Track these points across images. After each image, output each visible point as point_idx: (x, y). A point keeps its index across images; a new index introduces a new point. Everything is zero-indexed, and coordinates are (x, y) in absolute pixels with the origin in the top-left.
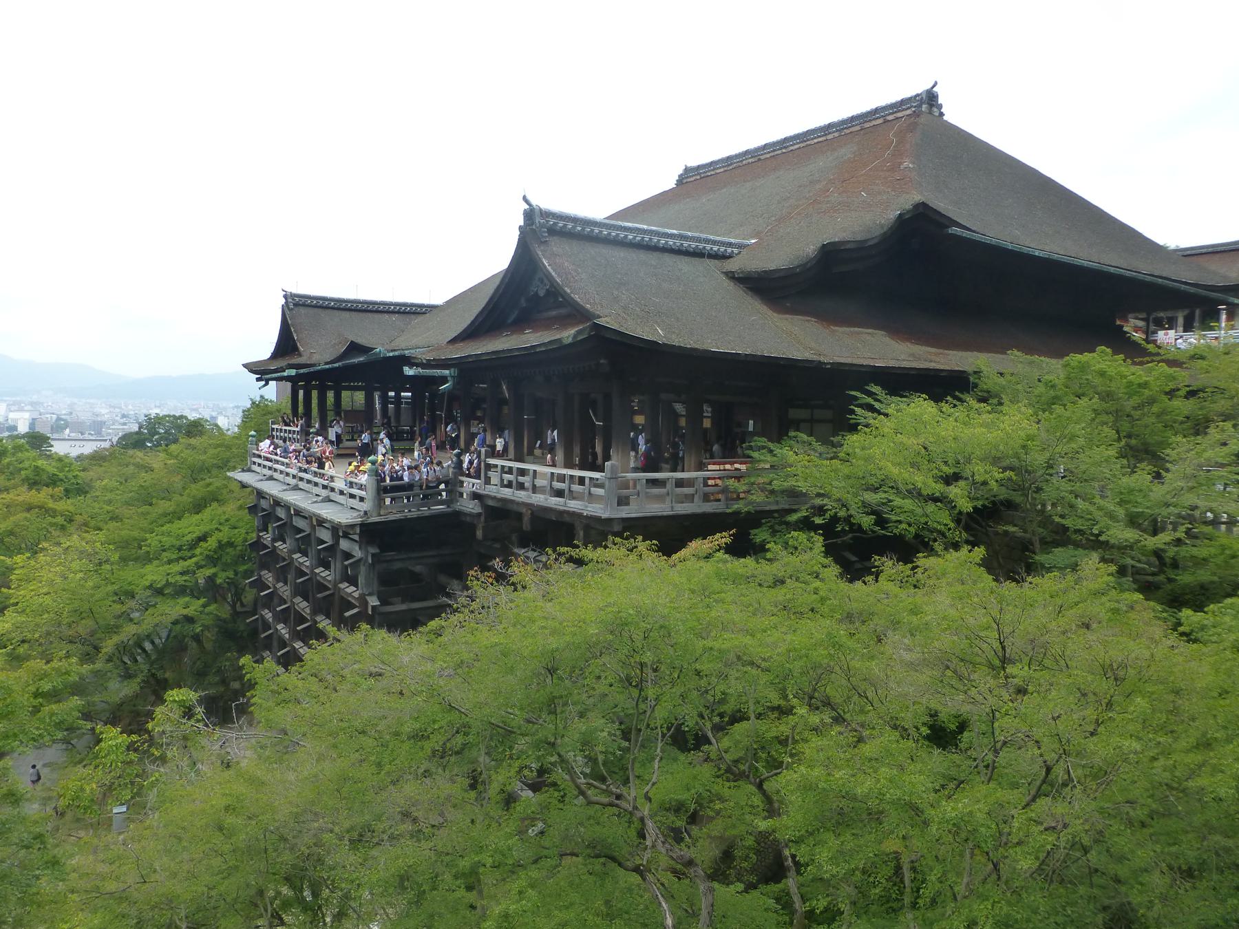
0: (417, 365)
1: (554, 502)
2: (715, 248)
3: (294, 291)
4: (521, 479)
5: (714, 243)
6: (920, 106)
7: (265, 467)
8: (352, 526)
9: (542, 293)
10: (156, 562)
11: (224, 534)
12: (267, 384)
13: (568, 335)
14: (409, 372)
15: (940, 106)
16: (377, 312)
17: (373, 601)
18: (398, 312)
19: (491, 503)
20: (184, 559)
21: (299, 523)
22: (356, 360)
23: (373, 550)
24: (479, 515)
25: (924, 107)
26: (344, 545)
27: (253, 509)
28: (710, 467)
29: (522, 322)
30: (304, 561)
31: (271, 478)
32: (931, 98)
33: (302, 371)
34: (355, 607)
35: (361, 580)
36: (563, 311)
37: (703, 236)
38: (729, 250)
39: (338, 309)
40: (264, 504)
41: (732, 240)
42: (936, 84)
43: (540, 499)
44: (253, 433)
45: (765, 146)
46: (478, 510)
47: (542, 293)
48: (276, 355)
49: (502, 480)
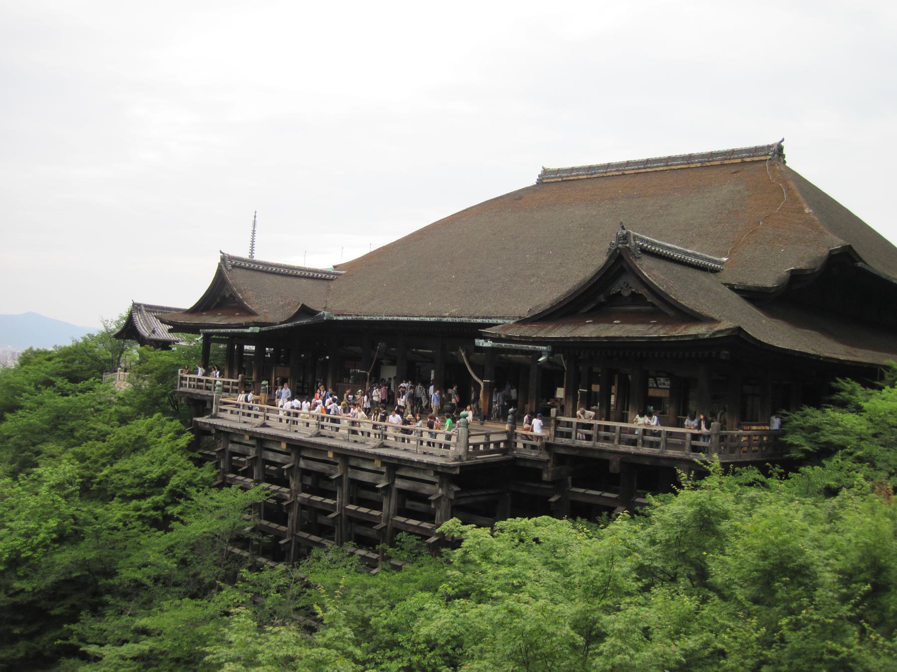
1: (646, 450)
5: (709, 260)
7: (243, 414)
8: (454, 468)
9: (626, 294)
14: (480, 343)
15: (784, 156)
16: (296, 276)
19: (562, 451)
22: (304, 321)
23: (456, 489)
24: (548, 461)
26: (399, 484)
28: (745, 428)
31: (264, 425)
33: (264, 329)
39: (266, 272)
42: (783, 140)
43: (632, 449)
45: (628, 163)
46: (545, 456)
47: (626, 294)
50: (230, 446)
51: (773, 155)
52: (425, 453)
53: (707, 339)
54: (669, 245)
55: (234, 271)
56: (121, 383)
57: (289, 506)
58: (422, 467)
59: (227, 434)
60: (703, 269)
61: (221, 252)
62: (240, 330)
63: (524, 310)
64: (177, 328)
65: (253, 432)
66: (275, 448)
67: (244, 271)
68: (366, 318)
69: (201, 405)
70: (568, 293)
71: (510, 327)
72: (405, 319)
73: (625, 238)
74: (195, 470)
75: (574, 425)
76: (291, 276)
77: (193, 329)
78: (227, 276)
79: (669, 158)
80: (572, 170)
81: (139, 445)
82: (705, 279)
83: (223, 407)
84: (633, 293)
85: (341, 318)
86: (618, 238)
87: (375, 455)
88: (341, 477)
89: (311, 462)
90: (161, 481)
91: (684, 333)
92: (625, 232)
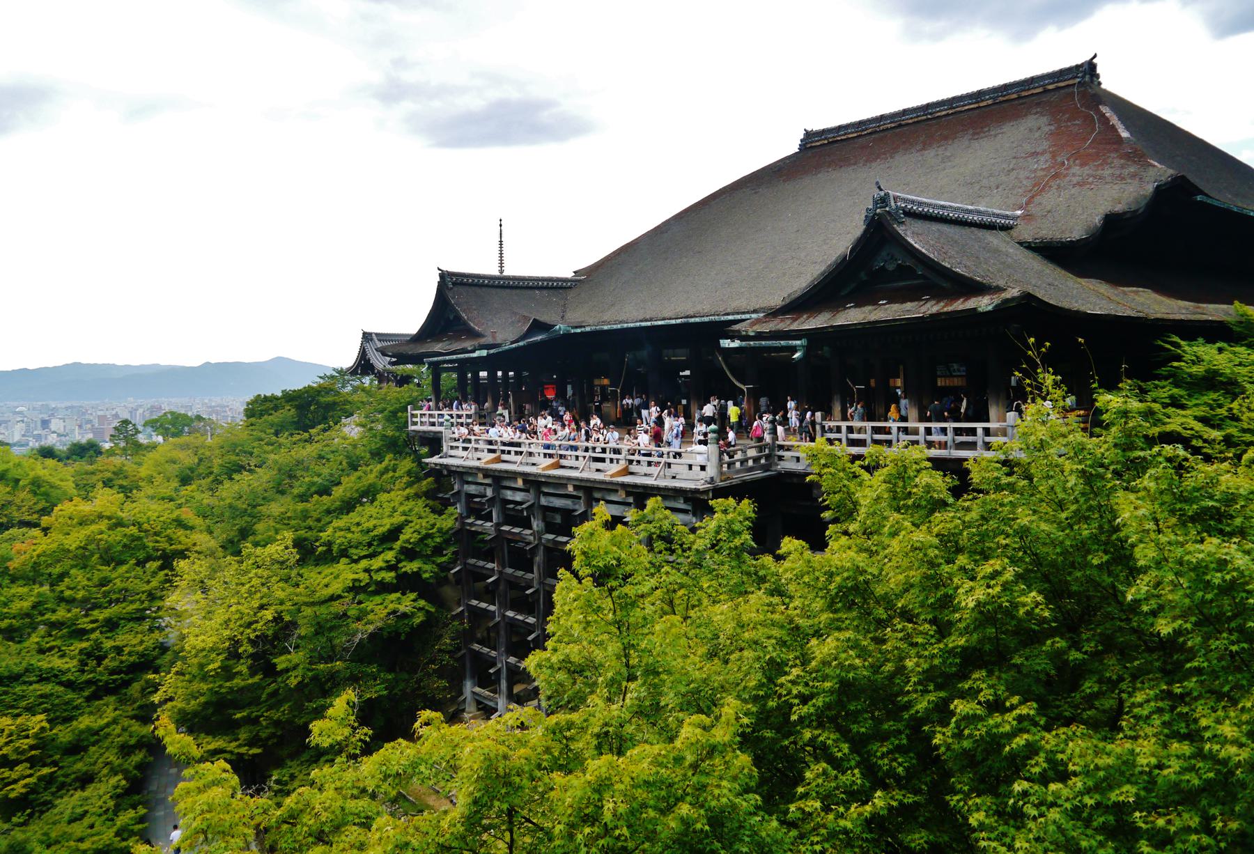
0: (732, 338)
5: (998, 216)
6: (1083, 77)
9: (891, 267)
13: (984, 303)
14: (726, 343)
15: (1098, 76)
16: (528, 288)
18: (547, 288)
25: (1087, 78)
29: (864, 298)
31: (498, 460)
32: (1089, 68)
33: (492, 351)
42: (1095, 56)
45: (905, 112)
47: (891, 267)
49: (848, 439)
50: (466, 487)
51: (1083, 77)
54: (942, 203)
56: (351, 430)
57: (534, 551)
58: (670, 493)
59: (464, 474)
60: (991, 227)
62: (467, 355)
63: (776, 301)
64: (402, 359)
65: (487, 470)
66: (513, 485)
67: (467, 288)
68: (606, 328)
69: (434, 443)
70: (822, 274)
71: (758, 321)
72: (649, 324)
73: (884, 200)
74: (432, 518)
75: (844, 429)
76: (521, 288)
77: (417, 360)
79: (954, 99)
80: (840, 128)
81: (370, 494)
82: (994, 239)
83: (455, 444)
84: (899, 265)
85: (579, 331)
86: (875, 202)
87: (617, 484)
89: (552, 499)
90: (394, 534)
91: (961, 307)
92: (882, 193)
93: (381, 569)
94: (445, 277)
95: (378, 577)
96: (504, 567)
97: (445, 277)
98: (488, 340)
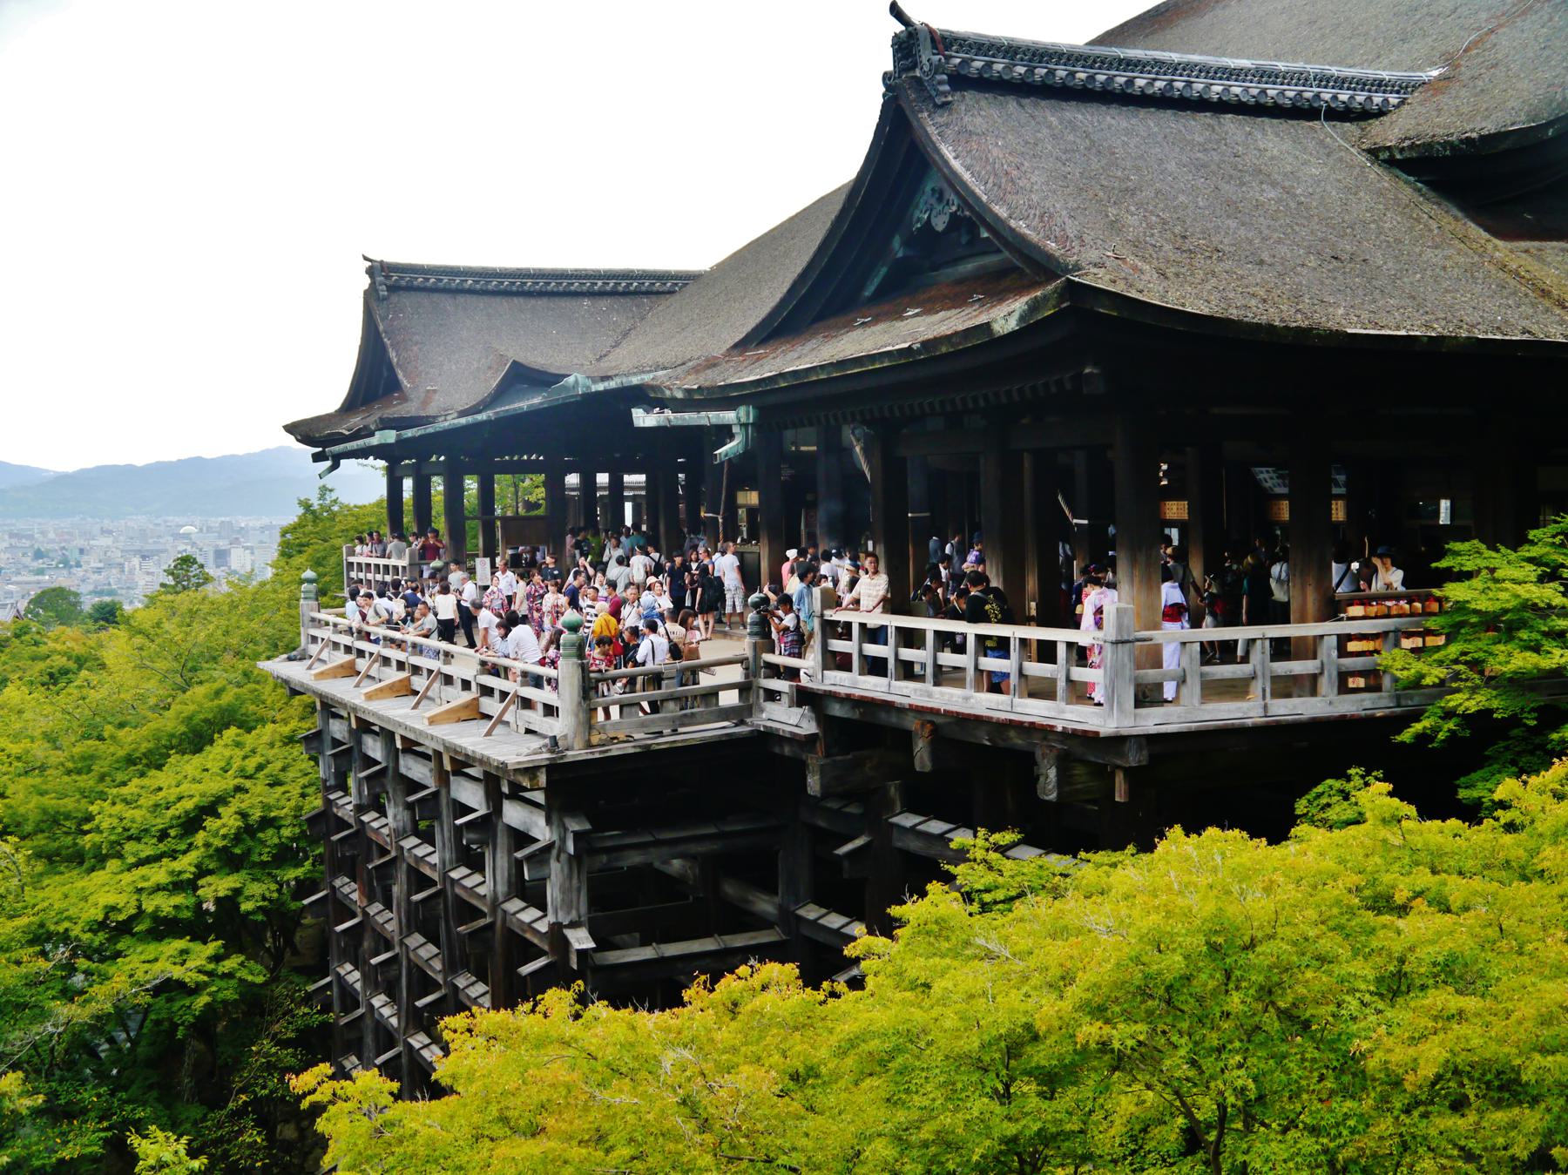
1: (984, 704)
2: (1344, 96)
3: (390, 258)
4: (907, 654)
5: (1341, 83)
8: (531, 771)
9: (940, 224)
10: (113, 864)
11: (257, 799)
12: (335, 466)
14: (643, 418)
17: (580, 940)
18: (614, 293)
19: (837, 710)
20: (173, 854)
21: (416, 770)
23: (574, 825)
24: (812, 738)
26: (514, 814)
27: (314, 740)
30: (432, 857)
33: (409, 433)
34: (540, 953)
35: (552, 893)
36: (990, 260)
37: (1313, 68)
38: (1378, 99)
40: (338, 729)
41: (1385, 75)
44: (309, 574)
46: (809, 727)
47: (940, 224)
48: (350, 406)
49: (863, 657)
52: (528, 731)
53: (1012, 335)
55: (394, 298)
61: (366, 259)
68: (635, 380)
76: (541, 294)
78: (378, 314)
85: (601, 387)
88: (436, 795)
93: (159, 888)
94: (377, 270)
95: (149, 906)
96: (371, 901)
97: (377, 270)
98: (410, 409)
